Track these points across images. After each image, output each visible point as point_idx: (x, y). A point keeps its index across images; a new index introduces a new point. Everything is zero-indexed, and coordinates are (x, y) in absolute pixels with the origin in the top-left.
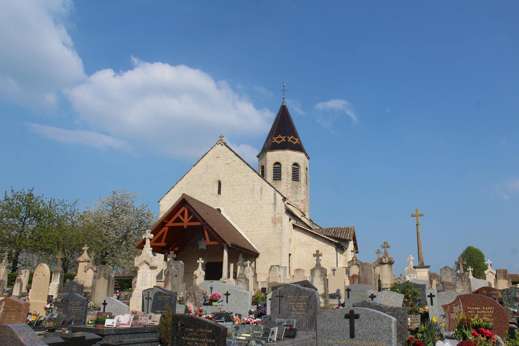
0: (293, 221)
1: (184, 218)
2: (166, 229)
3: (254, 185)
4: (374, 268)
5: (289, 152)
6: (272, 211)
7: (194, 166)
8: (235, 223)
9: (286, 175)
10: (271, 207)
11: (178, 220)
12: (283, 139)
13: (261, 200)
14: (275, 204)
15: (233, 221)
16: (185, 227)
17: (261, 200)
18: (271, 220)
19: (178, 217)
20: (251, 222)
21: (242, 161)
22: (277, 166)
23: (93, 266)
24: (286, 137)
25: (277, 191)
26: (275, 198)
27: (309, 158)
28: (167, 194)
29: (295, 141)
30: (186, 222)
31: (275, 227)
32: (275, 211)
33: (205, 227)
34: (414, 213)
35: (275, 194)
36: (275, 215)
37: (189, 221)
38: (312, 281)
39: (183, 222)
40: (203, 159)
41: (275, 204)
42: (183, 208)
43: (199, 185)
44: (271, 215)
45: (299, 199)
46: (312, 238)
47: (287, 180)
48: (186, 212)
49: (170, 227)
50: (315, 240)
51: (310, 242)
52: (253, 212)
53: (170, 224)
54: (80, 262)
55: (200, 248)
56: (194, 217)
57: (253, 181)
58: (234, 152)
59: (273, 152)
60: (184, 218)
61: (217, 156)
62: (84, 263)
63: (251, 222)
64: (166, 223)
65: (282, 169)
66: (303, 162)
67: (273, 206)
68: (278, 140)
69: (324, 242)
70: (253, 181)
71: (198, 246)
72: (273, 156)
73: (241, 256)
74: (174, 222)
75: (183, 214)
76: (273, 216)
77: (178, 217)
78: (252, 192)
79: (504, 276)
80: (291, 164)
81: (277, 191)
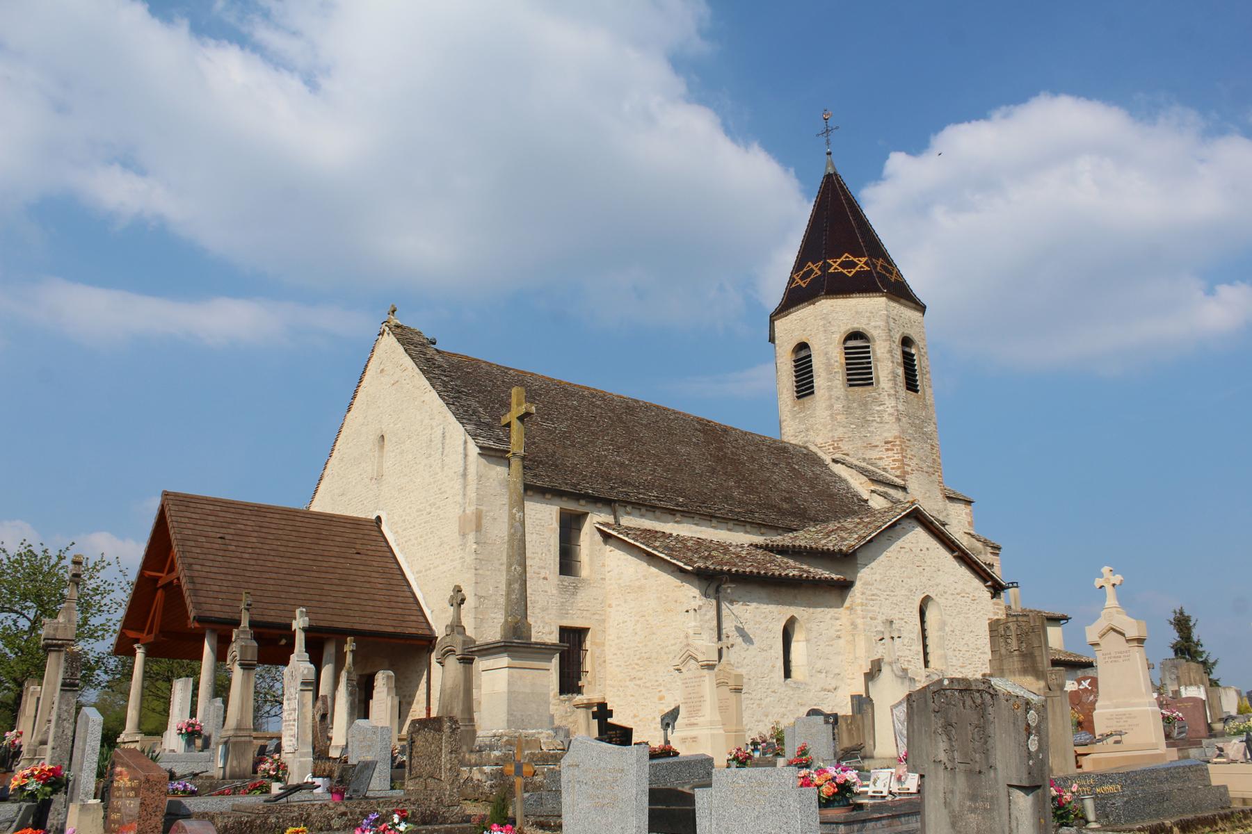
0: (597, 518)
6: (459, 498)
7: (349, 410)
8: (402, 551)
9: (823, 374)
10: (458, 485)
22: (803, 354)
26: (466, 455)
27: (921, 308)
29: (854, 265)
31: (464, 545)
35: (466, 442)
38: (900, 703)
40: (363, 384)
41: (464, 475)
45: (877, 440)
47: (830, 388)
50: (653, 570)
66: (882, 324)
67: (461, 480)
69: (672, 573)
72: (792, 327)
80: (838, 337)
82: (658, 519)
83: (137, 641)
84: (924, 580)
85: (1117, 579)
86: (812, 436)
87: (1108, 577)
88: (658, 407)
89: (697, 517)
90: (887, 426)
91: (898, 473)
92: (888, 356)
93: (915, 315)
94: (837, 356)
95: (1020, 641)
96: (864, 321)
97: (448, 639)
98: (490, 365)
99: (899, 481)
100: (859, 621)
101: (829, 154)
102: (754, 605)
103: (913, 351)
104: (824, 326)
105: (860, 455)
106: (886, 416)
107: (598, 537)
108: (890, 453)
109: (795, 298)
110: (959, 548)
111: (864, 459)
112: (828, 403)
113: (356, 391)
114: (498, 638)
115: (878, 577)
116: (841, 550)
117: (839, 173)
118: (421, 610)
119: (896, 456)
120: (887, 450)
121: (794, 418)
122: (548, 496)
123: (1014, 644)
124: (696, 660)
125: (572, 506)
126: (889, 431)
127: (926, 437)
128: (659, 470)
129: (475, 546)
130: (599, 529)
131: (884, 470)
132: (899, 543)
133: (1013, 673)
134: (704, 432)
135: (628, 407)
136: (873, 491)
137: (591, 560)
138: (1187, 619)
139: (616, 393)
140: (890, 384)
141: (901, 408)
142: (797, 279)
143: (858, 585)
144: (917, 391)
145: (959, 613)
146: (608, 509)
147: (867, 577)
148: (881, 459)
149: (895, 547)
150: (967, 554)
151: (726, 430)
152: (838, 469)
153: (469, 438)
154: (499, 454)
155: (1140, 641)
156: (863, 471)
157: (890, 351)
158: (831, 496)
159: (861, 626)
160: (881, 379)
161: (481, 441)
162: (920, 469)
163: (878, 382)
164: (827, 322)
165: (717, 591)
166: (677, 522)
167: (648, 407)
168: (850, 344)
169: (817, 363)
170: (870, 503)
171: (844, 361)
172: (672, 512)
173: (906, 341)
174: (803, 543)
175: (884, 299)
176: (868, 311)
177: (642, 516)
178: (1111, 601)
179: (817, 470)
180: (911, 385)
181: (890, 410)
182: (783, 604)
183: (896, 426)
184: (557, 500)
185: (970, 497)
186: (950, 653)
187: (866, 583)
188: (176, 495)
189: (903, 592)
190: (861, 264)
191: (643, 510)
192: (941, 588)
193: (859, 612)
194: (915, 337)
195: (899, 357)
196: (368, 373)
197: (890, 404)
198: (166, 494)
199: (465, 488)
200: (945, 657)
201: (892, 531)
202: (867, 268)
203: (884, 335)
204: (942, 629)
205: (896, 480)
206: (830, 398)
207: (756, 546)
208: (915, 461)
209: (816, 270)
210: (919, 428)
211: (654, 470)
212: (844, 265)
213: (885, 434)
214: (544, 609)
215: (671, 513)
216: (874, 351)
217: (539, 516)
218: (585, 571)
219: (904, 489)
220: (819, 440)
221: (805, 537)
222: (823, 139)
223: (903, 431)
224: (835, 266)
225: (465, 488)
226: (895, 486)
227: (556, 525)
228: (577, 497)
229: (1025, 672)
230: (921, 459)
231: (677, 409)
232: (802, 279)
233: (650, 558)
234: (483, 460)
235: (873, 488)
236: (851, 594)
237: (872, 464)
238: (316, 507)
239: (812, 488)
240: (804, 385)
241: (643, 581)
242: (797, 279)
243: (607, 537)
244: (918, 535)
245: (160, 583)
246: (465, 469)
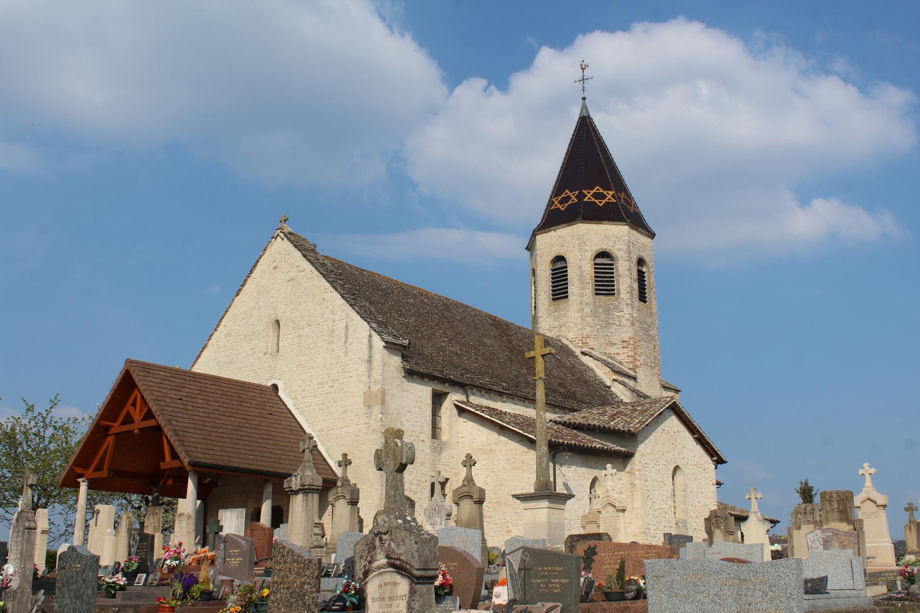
0: (455, 397)
2: (110, 440)
3: (334, 321)
4: (457, 504)
5: (582, 229)
6: (364, 378)
7: (237, 295)
8: (301, 413)
9: (577, 283)
10: (363, 368)
11: (129, 420)
15: (298, 409)
18: (361, 400)
20: (328, 408)
21: (314, 269)
22: (559, 265)
24: (581, 192)
26: (371, 346)
27: (652, 235)
28: (195, 362)
29: (604, 197)
31: (369, 415)
32: (370, 376)
35: (370, 336)
36: (369, 388)
37: (143, 419)
40: (253, 275)
41: (370, 361)
44: (363, 388)
46: (495, 435)
47: (581, 295)
48: (139, 398)
51: (494, 446)
52: (331, 384)
53: (117, 428)
57: (333, 313)
59: (550, 233)
61: (275, 264)
63: (328, 408)
64: (108, 428)
65: (569, 272)
66: (624, 247)
67: (367, 365)
69: (520, 442)
70: (333, 313)
73: (269, 489)
75: (134, 404)
79: (841, 512)
80: (590, 255)
82: (491, 399)
83: (81, 476)
84: (676, 454)
85: (873, 471)
86: (564, 331)
87: (867, 470)
88: (462, 305)
89: (516, 398)
90: (625, 329)
91: (631, 366)
92: (628, 273)
93: (644, 240)
94: (589, 270)
95: (839, 504)
96: (611, 244)
97: (465, 489)
98: (351, 266)
99: (631, 373)
100: (637, 482)
102: (574, 467)
103: (644, 270)
104: (579, 245)
105: (602, 350)
106: (624, 321)
107: (455, 411)
108: (626, 350)
109: (553, 219)
110: (698, 431)
111: (605, 354)
112: (579, 307)
113: (245, 281)
114: (533, 491)
115: (649, 451)
116: (629, 431)
117: (592, 116)
118: (325, 460)
119: (630, 353)
120: (623, 347)
121: (550, 315)
122: (426, 380)
123: (835, 505)
124: (615, 507)
125: (440, 388)
126: (625, 332)
127: (650, 338)
128: (480, 359)
129: (380, 416)
130: (456, 406)
131: (620, 363)
132: (662, 427)
133: (834, 520)
134: (495, 326)
135: (445, 305)
136: (614, 380)
137: (450, 428)
138: (811, 489)
139: (434, 292)
140: (628, 296)
141: (635, 315)
142: (556, 203)
143: (637, 456)
144: (645, 302)
145: (696, 479)
146: (461, 391)
147: (644, 450)
148: (618, 354)
149: (659, 429)
150: (703, 436)
151: (508, 325)
152: (586, 360)
153: (375, 335)
154: (397, 347)
155: (884, 506)
156: (607, 364)
157: (629, 270)
158: (586, 382)
159: (638, 486)
160: (622, 291)
161: (386, 337)
162: (646, 364)
163: (619, 294)
164: (581, 241)
165: (554, 457)
166: (503, 402)
167: (457, 305)
168: (599, 261)
169: (572, 274)
170: (613, 389)
171: (593, 274)
172: (501, 394)
173: (641, 262)
174: (620, 426)
175: (627, 227)
176: (612, 235)
177: (482, 396)
178: (868, 483)
179: (571, 359)
180: (642, 298)
181: (627, 316)
182: (591, 467)
183: (631, 329)
184: (431, 383)
185: (678, 387)
186: (690, 508)
187: (642, 455)
188: (137, 362)
189: (663, 462)
190: (609, 196)
191: (483, 392)
192: (685, 460)
193: (637, 475)
194: (647, 259)
195: (635, 275)
196: (258, 267)
197: (627, 311)
198: (129, 362)
199: (370, 371)
200: (686, 510)
201: (659, 419)
202: (613, 200)
203: (625, 256)
204: (685, 490)
205: (629, 371)
206: (581, 303)
207: (555, 422)
208: (643, 357)
209: (573, 198)
210: (646, 331)
211: (477, 359)
212: (596, 196)
213: (623, 335)
214: (422, 464)
215: (500, 395)
216: (617, 269)
217: (419, 394)
218: (444, 437)
219: (635, 379)
220: (571, 336)
221: (577, 418)
222: (580, 85)
223: (636, 334)
224: (589, 196)
225: (370, 371)
226: (629, 377)
227: (429, 401)
228: (443, 380)
229: (841, 520)
230: (647, 356)
231: (475, 307)
232: (560, 203)
233: (502, 430)
234: (386, 352)
235: (614, 377)
236: (631, 462)
237: (611, 358)
238: (199, 368)
239: (573, 375)
240: (560, 290)
241: (494, 446)
242: (556, 203)
243: (461, 411)
244: (673, 422)
245: (112, 431)
246: (370, 357)
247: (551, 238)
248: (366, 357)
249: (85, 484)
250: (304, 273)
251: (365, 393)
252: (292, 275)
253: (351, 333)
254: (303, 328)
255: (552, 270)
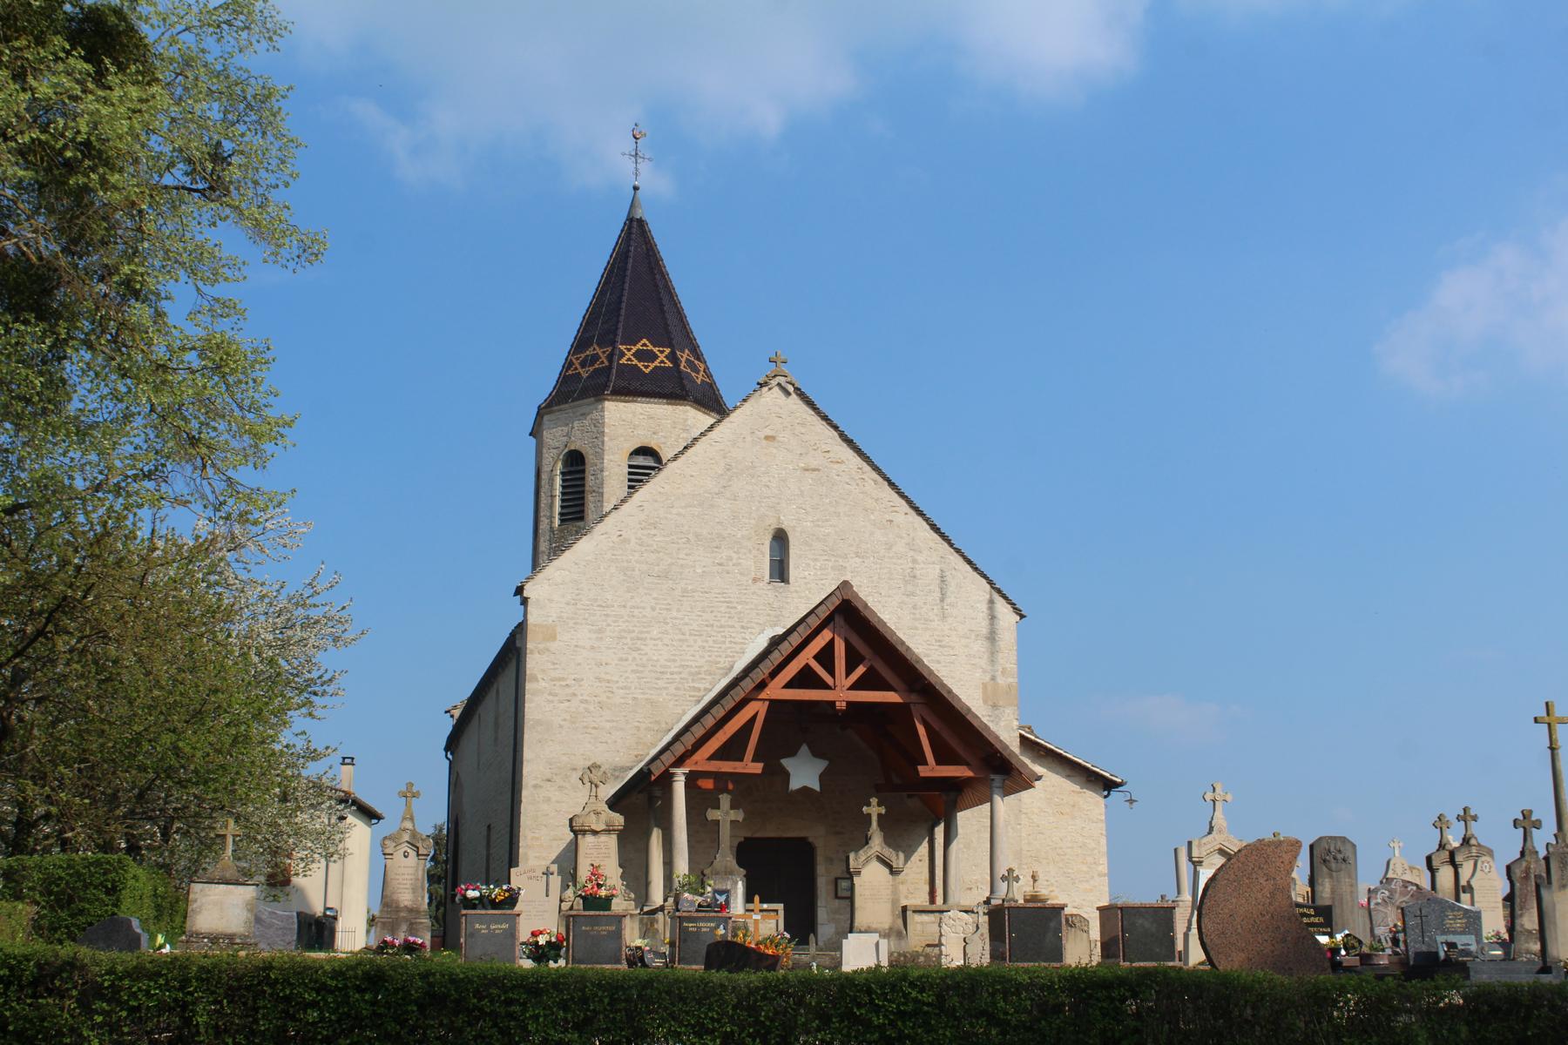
1: (832, 673)
2: (757, 708)
3: (914, 561)
6: (984, 662)
10: (980, 646)
12: (662, 357)
13: (944, 617)
14: (992, 637)
16: (841, 705)
17: (944, 617)
19: (807, 667)
21: (867, 468)
22: (641, 461)
23: (888, 853)
25: (999, 591)
26: (993, 618)
30: (842, 691)
32: (992, 662)
33: (917, 712)
34: (1558, 712)
35: (991, 602)
36: (993, 678)
37: (853, 687)
39: (826, 687)
41: (992, 637)
42: (826, 635)
43: (697, 536)
49: (775, 705)
53: (776, 690)
54: (584, 832)
55: (795, 784)
56: (871, 671)
58: (836, 428)
60: (832, 673)
61: (770, 433)
62: (603, 838)
67: (986, 644)
68: (640, 355)
69: (1068, 777)
71: (786, 776)
74: (790, 685)
76: (987, 678)
77: (807, 667)
78: (910, 588)
81: (999, 591)
101: (636, 188)
247: (634, 413)
248: (985, 631)
249: (683, 778)
250: (843, 467)
251: (985, 686)
252: (814, 464)
253: (952, 588)
254: (845, 556)
255: (630, 467)
